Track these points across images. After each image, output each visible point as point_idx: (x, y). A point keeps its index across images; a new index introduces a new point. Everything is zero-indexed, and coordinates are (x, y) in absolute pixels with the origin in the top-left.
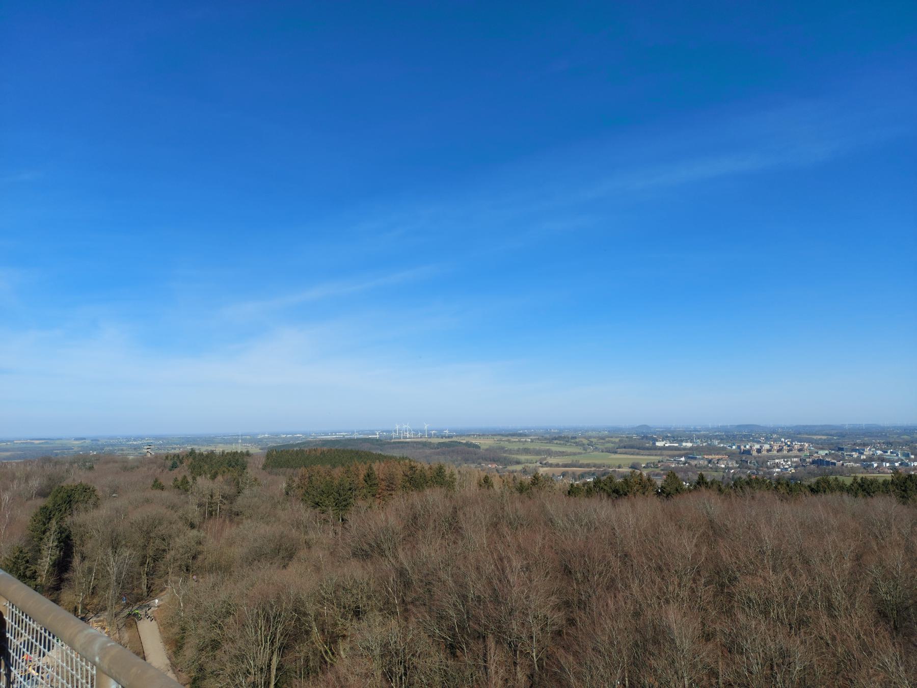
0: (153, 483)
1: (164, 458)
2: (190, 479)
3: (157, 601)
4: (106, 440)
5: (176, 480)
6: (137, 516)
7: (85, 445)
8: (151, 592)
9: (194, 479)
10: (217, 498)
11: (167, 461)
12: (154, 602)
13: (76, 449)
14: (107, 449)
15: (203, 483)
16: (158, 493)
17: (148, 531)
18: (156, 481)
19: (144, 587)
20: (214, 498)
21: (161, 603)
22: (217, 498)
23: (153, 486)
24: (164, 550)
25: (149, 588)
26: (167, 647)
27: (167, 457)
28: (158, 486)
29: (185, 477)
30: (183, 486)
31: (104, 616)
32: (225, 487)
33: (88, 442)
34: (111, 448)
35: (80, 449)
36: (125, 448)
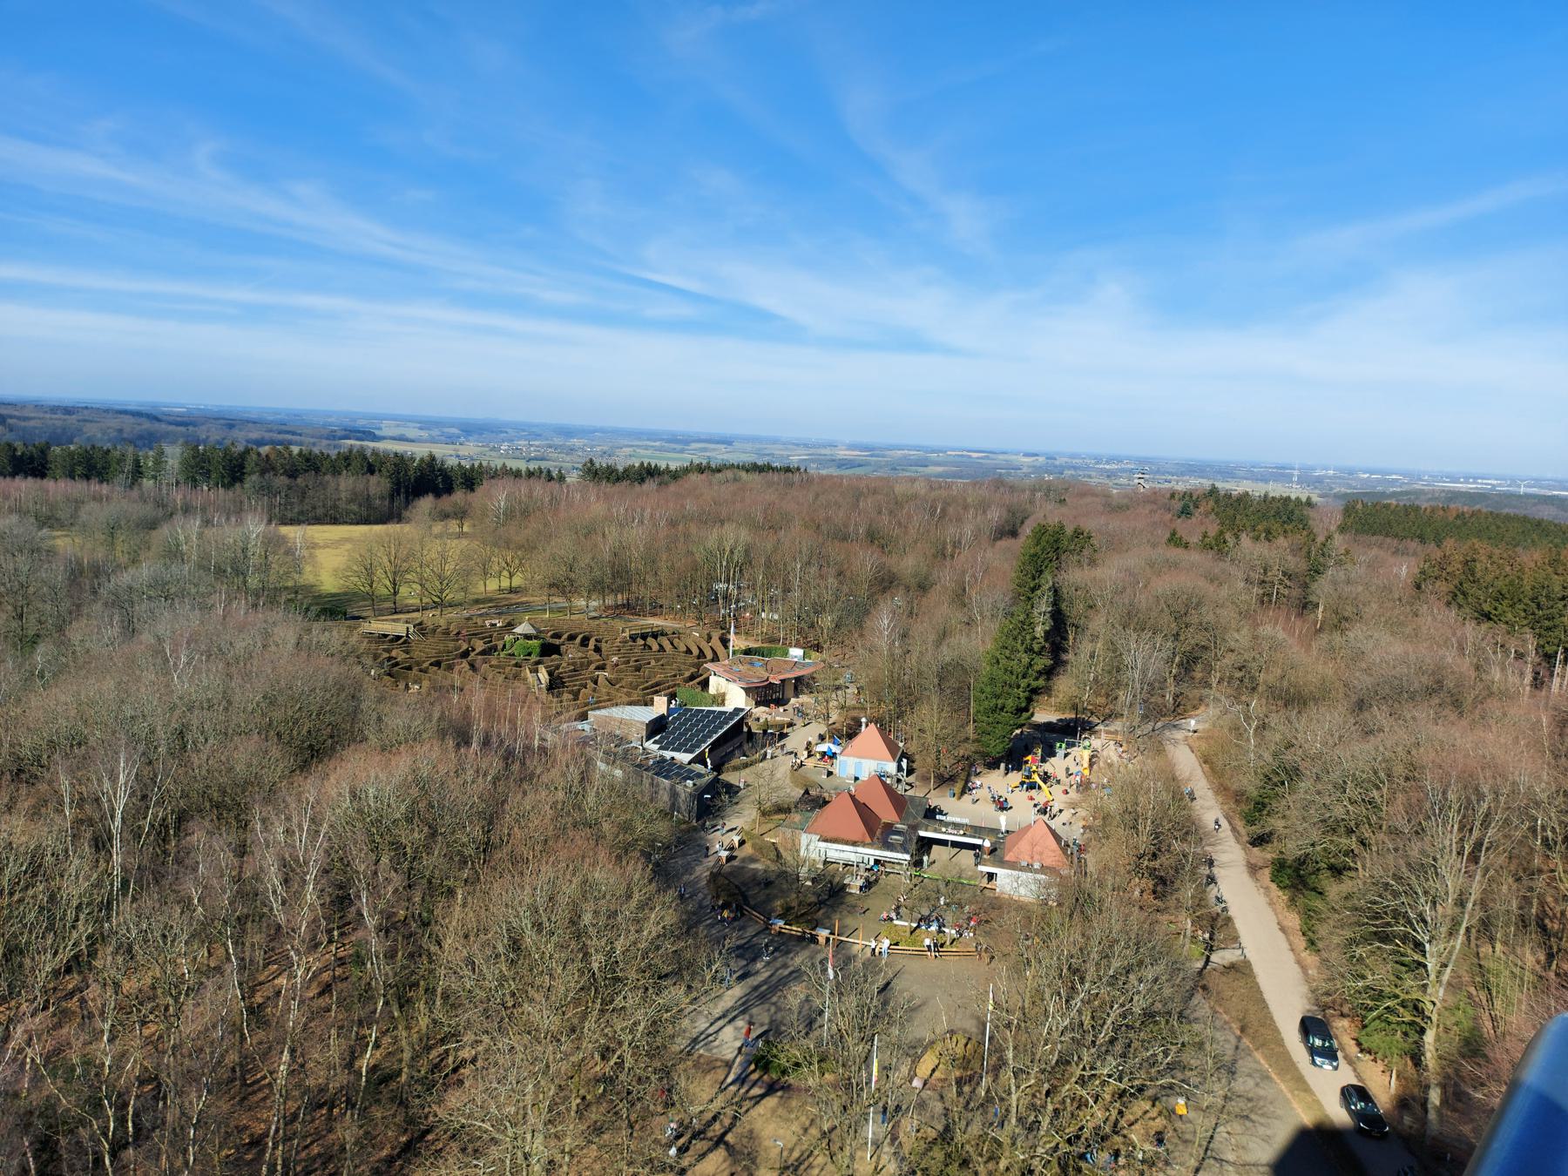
0: (1168, 535)
1: (1168, 496)
2: (1228, 536)
3: (1193, 722)
4: (1066, 459)
5: (1205, 536)
6: (1164, 585)
7: (1038, 464)
8: (1179, 709)
9: (1237, 537)
10: (1275, 574)
11: (1173, 502)
12: (1189, 724)
13: (1025, 470)
14: (1068, 473)
15: (1248, 547)
16: (1175, 553)
17: (1182, 612)
18: (1174, 534)
19: (1169, 698)
20: (1269, 574)
21: (1200, 727)
22: (1275, 574)
23: (1170, 540)
24: (1205, 648)
25: (1176, 696)
26: (1220, 800)
27: (1173, 496)
28: (1175, 540)
29: (1221, 533)
30: (1216, 546)
31: (1117, 725)
32: (1289, 558)
33: (1041, 459)
34: (1073, 472)
35: (1030, 470)
36: (1093, 474)
